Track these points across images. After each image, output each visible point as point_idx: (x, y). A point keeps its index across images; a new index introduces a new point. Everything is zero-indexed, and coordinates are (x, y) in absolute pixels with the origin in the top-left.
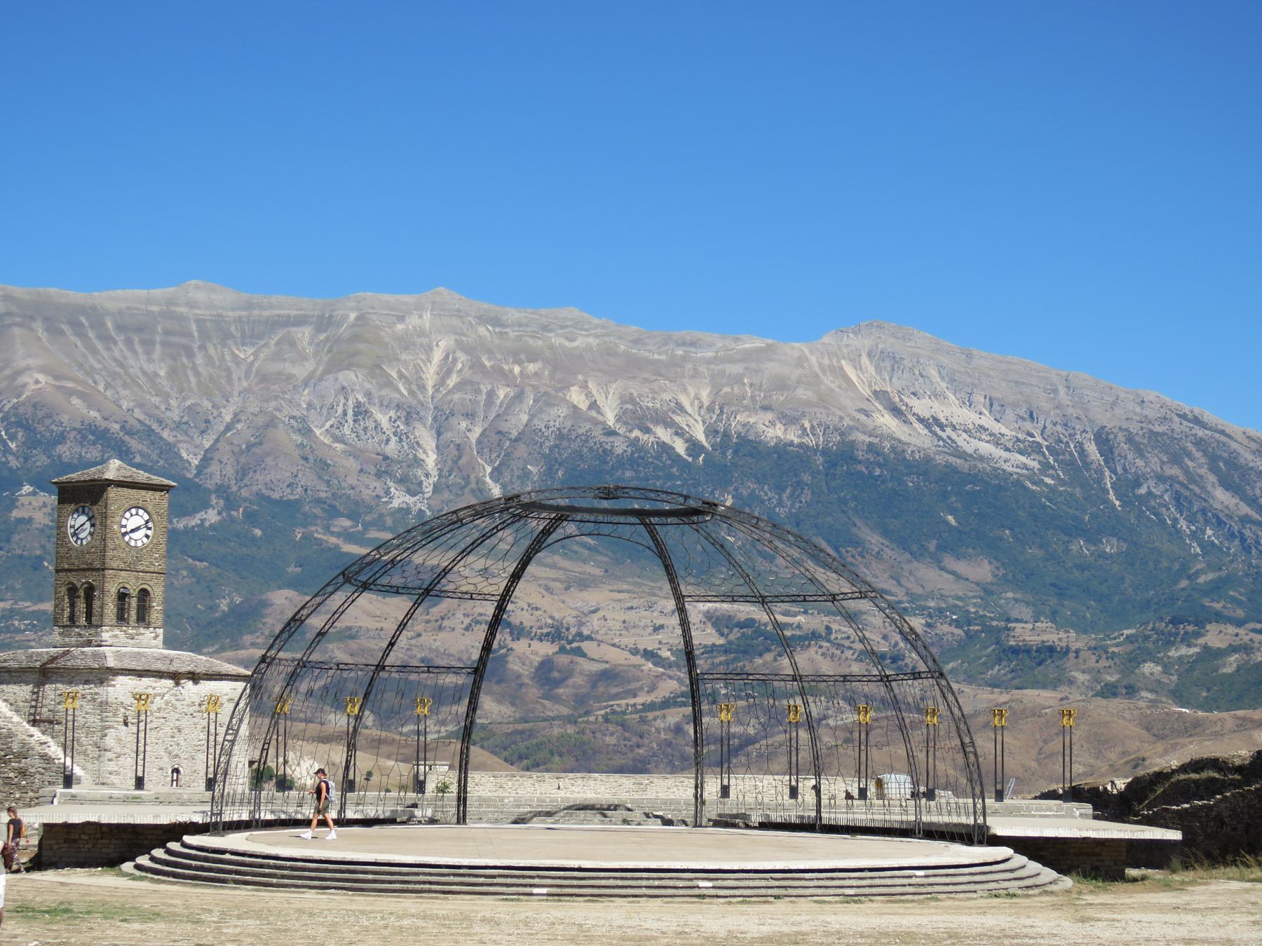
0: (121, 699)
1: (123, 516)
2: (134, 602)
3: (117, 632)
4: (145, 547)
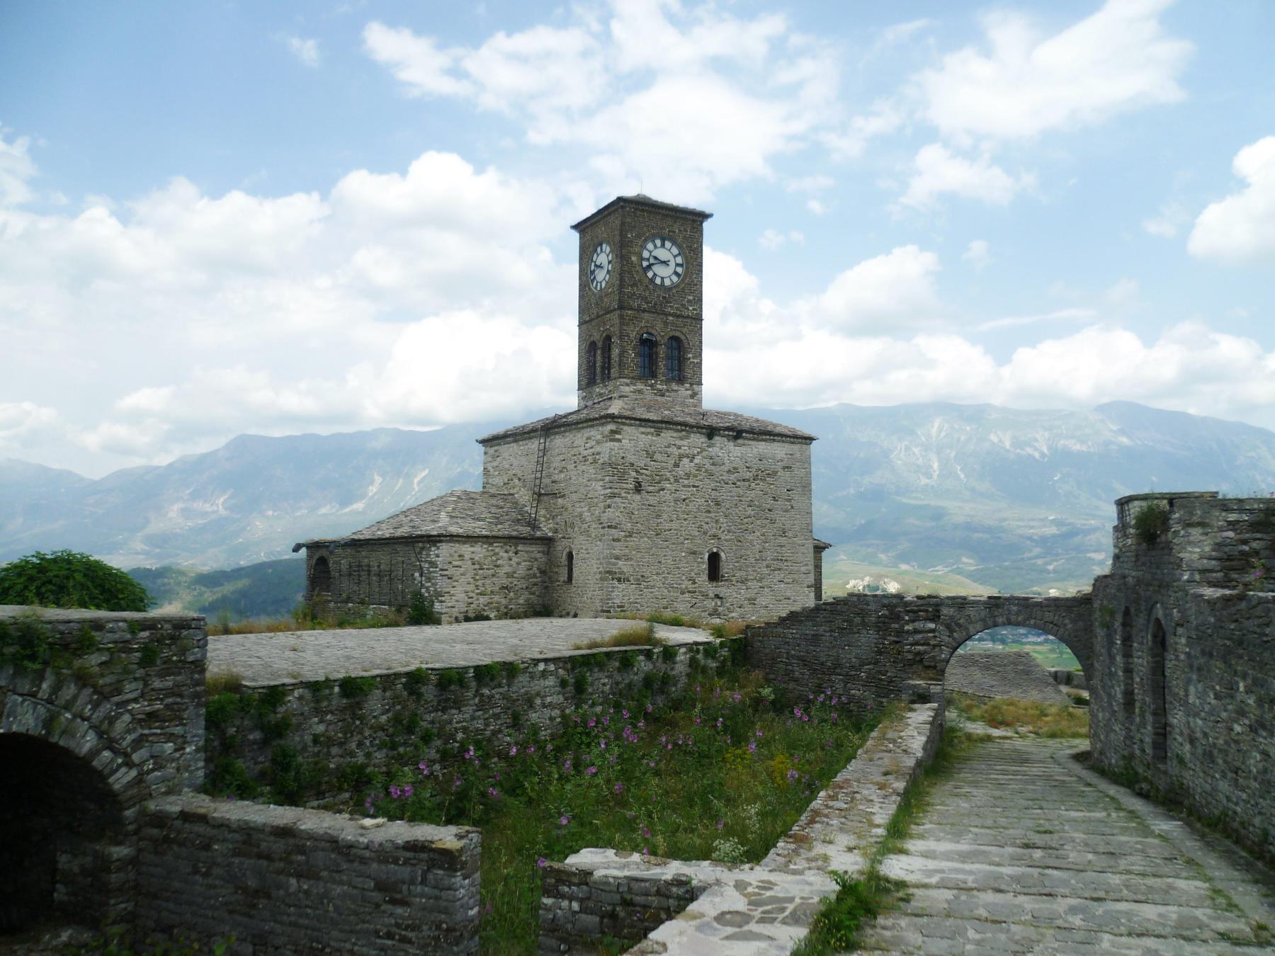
0: (631, 458)
3: (640, 386)
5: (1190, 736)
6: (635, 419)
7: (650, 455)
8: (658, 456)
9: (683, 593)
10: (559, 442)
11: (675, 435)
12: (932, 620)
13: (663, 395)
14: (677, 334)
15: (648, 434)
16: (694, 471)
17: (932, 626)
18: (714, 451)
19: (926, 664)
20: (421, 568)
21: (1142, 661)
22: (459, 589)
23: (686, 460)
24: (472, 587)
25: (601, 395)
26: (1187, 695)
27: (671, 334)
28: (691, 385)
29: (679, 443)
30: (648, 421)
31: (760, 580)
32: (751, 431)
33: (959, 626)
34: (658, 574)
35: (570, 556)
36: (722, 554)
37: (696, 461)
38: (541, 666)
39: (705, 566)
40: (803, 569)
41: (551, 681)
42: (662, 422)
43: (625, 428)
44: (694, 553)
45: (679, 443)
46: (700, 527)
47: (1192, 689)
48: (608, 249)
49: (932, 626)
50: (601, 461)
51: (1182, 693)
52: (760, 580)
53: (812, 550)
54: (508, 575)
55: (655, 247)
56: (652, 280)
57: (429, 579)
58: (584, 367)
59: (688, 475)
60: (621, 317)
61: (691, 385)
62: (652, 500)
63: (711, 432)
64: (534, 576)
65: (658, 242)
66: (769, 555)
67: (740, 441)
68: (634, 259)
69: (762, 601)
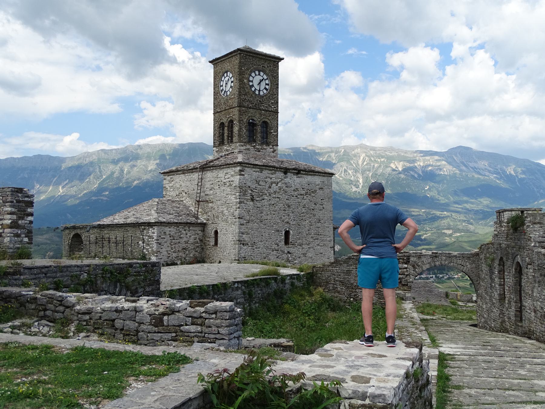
0: (249, 184)
2: (259, 129)
3: (248, 147)
4: (265, 95)
5: (534, 309)
6: (251, 164)
7: (258, 182)
8: (261, 183)
9: (273, 251)
10: (209, 175)
11: (269, 172)
12: (406, 263)
13: (259, 151)
14: (266, 120)
15: (256, 172)
16: (278, 190)
17: (406, 266)
18: (287, 180)
19: (403, 283)
20: (143, 239)
21: (510, 280)
22: (164, 249)
23: (274, 185)
24: (170, 249)
26: (533, 293)
27: (263, 120)
28: (273, 146)
29: (271, 176)
30: (257, 165)
31: (309, 244)
32: (305, 170)
33: (419, 266)
34: (261, 241)
35: (216, 233)
36: (291, 231)
37: (279, 185)
38: (236, 285)
39: (283, 237)
40: (328, 239)
41: (239, 292)
42: (263, 166)
43: (246, 169)
44: (278, 231)
45: (271, 176)
46: (281, 218)
47: (535, 290)
48: (231, 75)
49: (406, 266)
50: (234, 185)
51: (530, 292)
52: (309, 244)
53: (332, 229)
54: (186, 242)
55: (256, 75)
56: (254, 92)
57: (148, 245)
58: (217, 135)
59: (275, 192)
60: (240, 111)
61: (273, 146)
62: (258, 204)
63: (286, 171)
64: (197, 243)
65: (257, 73)
66: (313, 232)
67: (299, 175)
68: (245, 81)
69: (309, 255)
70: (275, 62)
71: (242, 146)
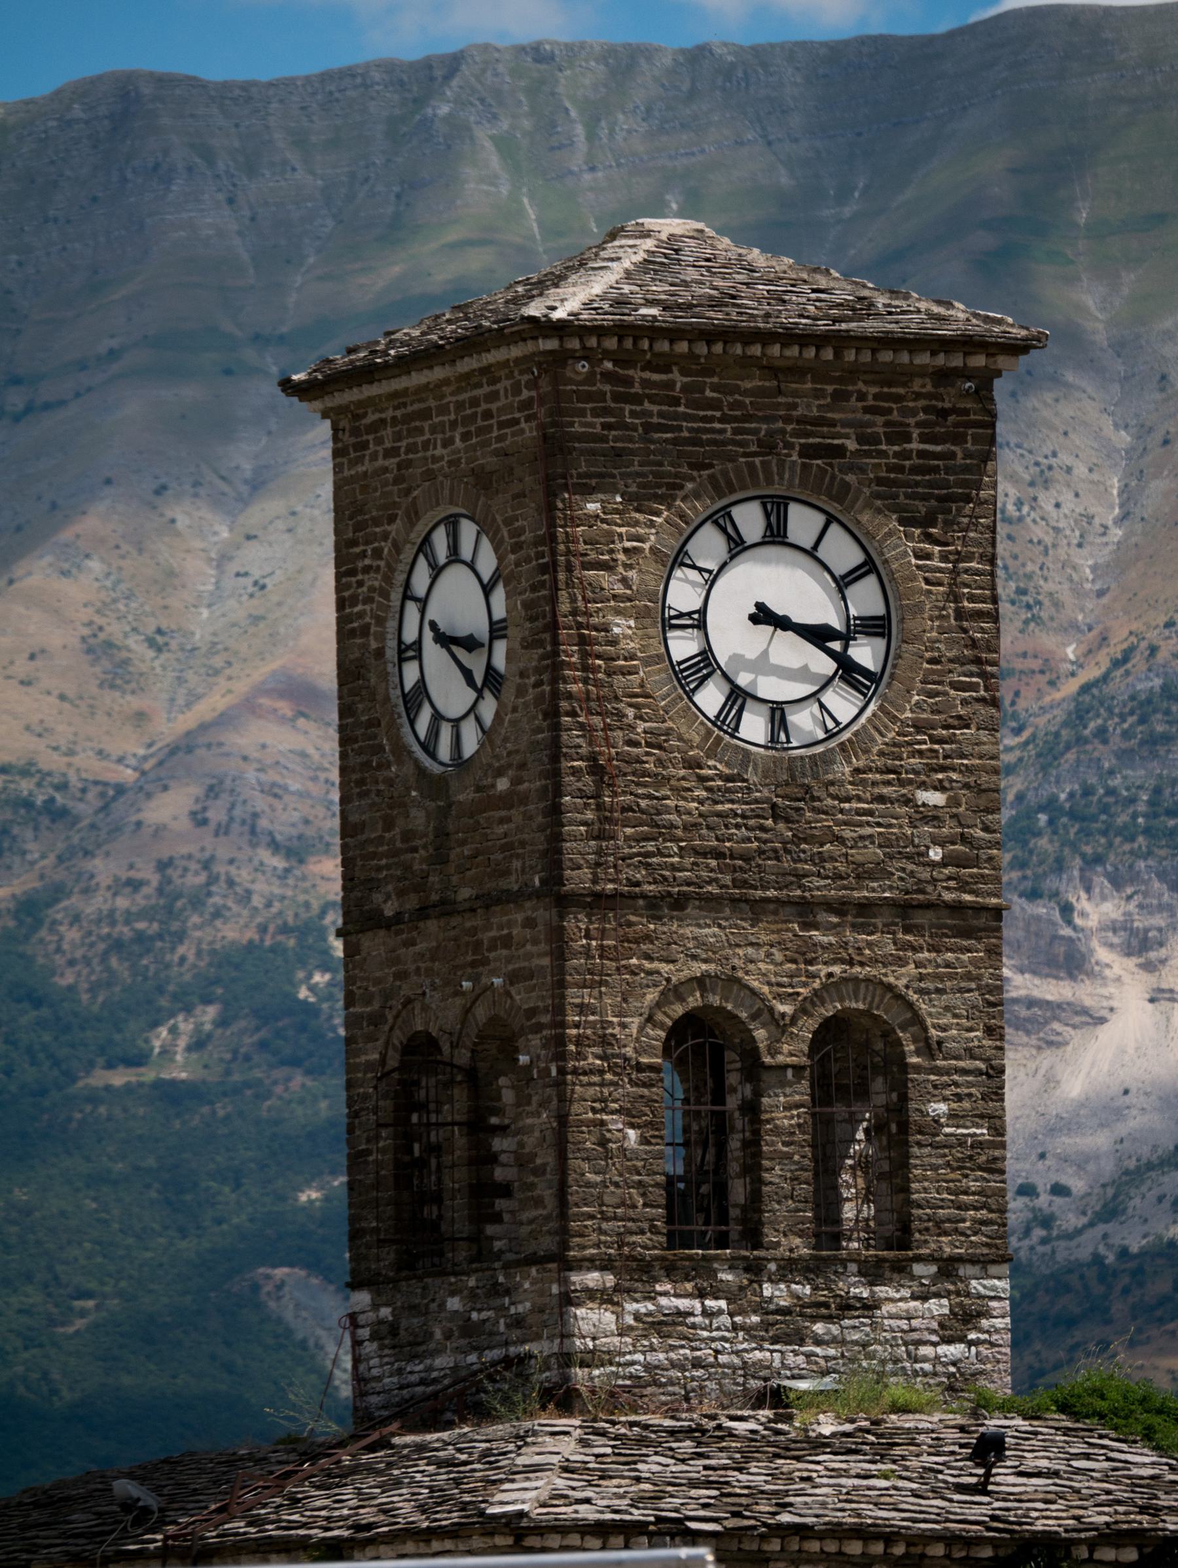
1: (680, 559)
3: (672, 1299)
25: (469, 1330)
28: (948, 1268)
48: (487, 563)
68: (621, 626)
70: (943, 376)
71: (604, 1297)
